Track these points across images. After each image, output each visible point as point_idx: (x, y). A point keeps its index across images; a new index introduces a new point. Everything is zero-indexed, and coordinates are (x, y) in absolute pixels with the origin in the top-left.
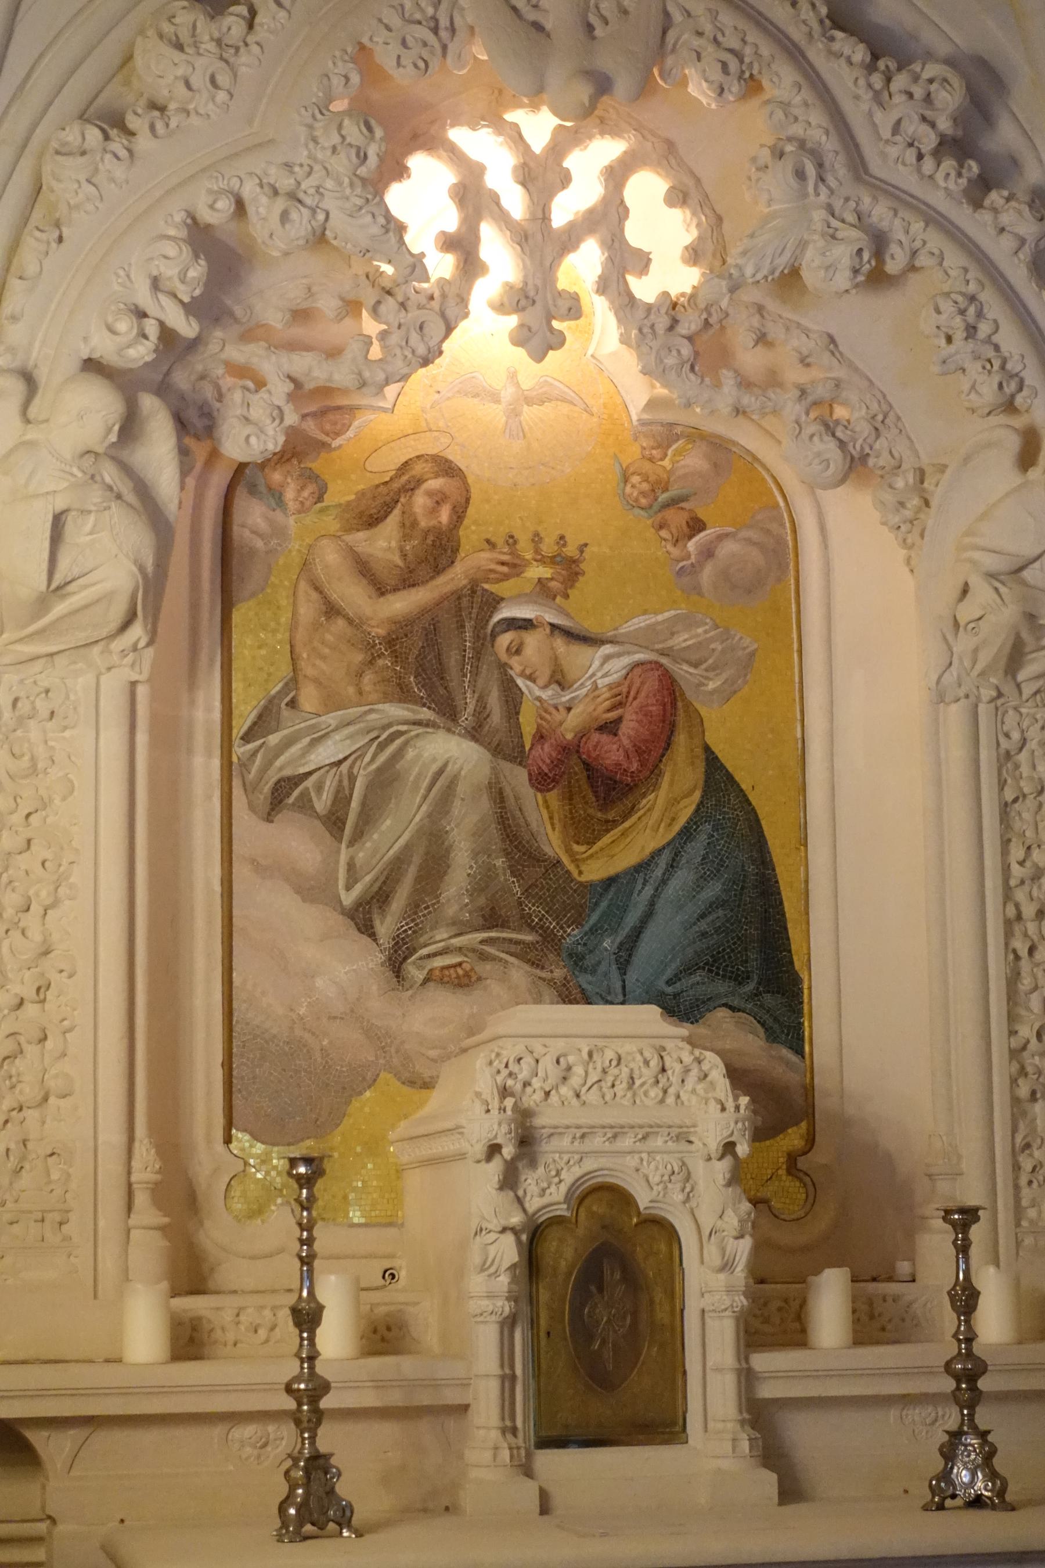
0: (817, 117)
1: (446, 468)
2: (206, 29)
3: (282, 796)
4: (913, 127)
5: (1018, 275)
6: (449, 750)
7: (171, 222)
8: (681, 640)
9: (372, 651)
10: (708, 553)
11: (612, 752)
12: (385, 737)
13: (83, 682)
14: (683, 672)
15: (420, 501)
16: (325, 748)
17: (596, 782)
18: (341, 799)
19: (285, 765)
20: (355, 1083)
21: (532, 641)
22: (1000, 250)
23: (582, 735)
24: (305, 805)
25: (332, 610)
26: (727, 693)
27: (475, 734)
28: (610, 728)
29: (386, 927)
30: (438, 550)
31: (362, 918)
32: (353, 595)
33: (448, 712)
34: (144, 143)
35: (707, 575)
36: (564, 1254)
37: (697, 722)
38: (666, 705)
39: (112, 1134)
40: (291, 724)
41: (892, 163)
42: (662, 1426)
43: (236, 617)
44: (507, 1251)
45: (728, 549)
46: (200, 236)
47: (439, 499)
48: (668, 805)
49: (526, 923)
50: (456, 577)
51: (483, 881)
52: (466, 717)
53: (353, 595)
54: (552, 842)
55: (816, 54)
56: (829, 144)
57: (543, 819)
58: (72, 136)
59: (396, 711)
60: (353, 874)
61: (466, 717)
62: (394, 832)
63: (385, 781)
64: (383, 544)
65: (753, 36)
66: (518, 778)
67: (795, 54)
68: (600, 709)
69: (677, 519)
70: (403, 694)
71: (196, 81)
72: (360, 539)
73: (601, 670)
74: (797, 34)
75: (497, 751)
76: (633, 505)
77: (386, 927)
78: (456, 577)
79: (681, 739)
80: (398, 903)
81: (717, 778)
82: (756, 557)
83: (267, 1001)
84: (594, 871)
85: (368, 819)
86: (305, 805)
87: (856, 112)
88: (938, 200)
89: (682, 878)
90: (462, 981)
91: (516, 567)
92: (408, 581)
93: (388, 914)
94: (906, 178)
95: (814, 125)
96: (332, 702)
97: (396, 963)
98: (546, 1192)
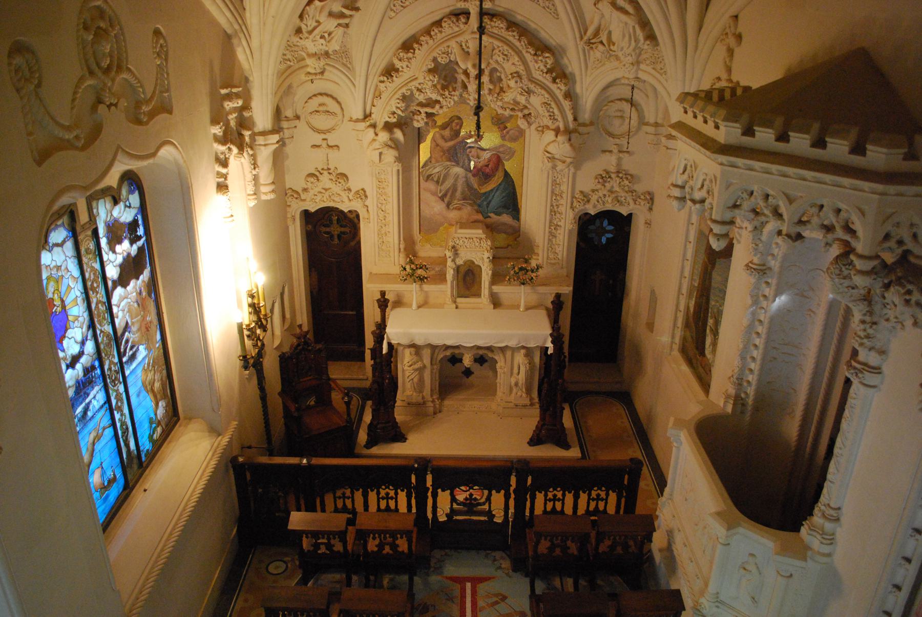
0: (522, 67)
1: (459, 118)
2: (406, 56)
3: (429, 178)
4: (542, 67)
5: (561, 98)
6: (457, 170)
7: (399, 95)
8: (501, 150)
9: (443, 151)
10: (508, 133)
11: (487, 170)
12: (447, 168)
13: (389, 169)
14: (501, 155)
15: (454, 124)
16: (437, 170)
17: (483, 174)
18: (439, 178)
19: (428, 173)
20: (442, 224)
21: (473, 150)
22: (557, 92)
23: (482, 167)
24: (432, 179)
25: (437, 145)
26: (508, 160)
27: (462, 167)
28: (487, 166)
29: (446, 200)
30: (457, 133)
31: (442, 198)
32: (441, 142)
33: (458, 164)
34: (394, 78)
35: (507, 137)
36: (462, 270)
37: (503, 165)
38: (497, 161)
39: (396, 241)
40: (430, 165)
41: (537, 75)
42: (478, 295)
43: (422, 146)
44: (452, 272)
45: (511, 132)
46: (404, 98)
47: (457, 124)
48: (498, 178)
49: (470, 199)
50: (459, 139)
51: (462, 194)
52: (461, 164)
53: (441, 142)
54: (476, 186)
55: (524, 52)
56: (523, 73)
57: (474, 182)
58: (382, 78)
59: (448, 163)
60: (441, 191)
61: (461, 164)
62: (448, 184)
63: (446, 176)
64: (447, 133)
65: (510, 51)
66: (470, 175)
67: (519, 53)
68: (485, 163)
69: (502, 126)
70: (450, 160)
71: (404, 66)
72: (442, 132)
73: (486, 156)
74: (520, 48)
75: (466, 170)
76: (493, 123)
77: (446, 200)
78: (459, 139)
79: (500, 168)
80: (449, 195)
81: (507, 174)
82: (517, 133)
83: (426, 212)
84: (483, 191)
85: (443, 182)
86: (432, 179)
87: (531, 64)
88: (546, 82)
89: (498, 193)
90: (459, 209)
91: (470, 137)
92: (451, 139)
93: (446, 198)
94: (540, 78)
95: (521, 69)
96: (437, 161)
97: (448, 206)
98: (460, 262)
